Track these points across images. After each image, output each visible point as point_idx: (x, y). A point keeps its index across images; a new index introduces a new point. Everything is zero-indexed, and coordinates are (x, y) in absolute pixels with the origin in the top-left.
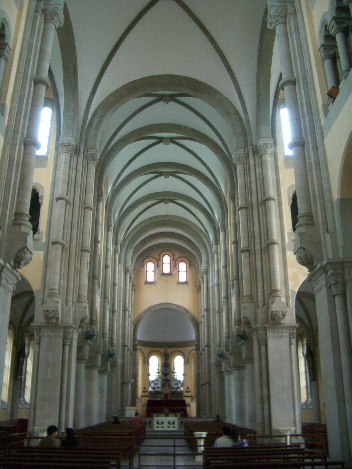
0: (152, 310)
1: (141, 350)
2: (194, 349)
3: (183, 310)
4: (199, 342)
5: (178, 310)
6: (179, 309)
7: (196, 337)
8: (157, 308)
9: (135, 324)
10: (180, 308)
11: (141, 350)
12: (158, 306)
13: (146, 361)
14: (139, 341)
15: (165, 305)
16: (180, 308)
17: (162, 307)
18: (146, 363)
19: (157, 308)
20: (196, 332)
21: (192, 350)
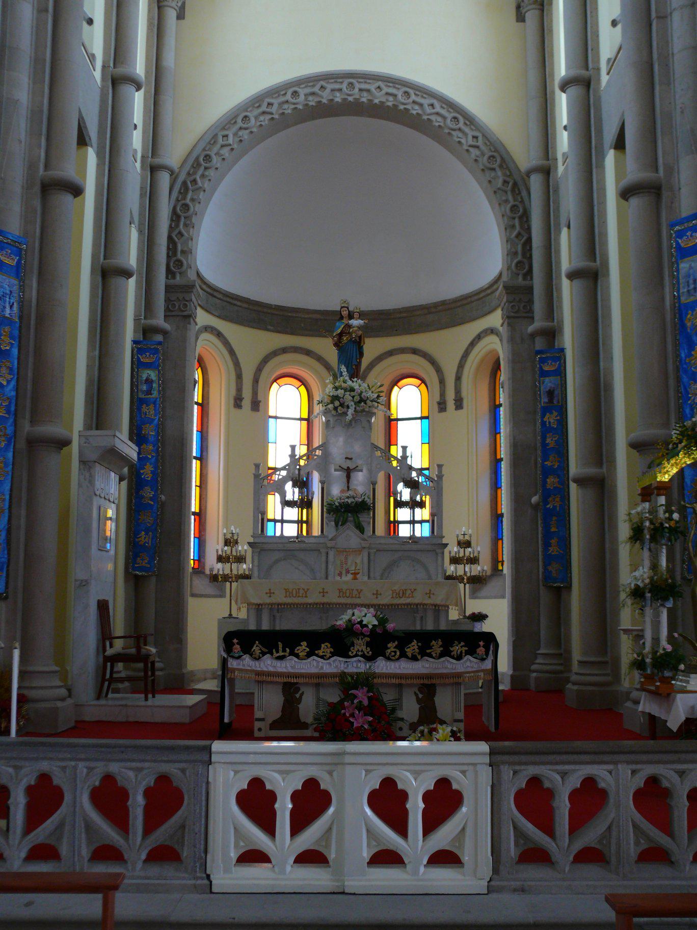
0: (274, 109)
1: (219, 335)
2: (492, 331)
3: (438, 108)
4: (529, 273)
5: (415, 110)
6: (421, 105)
7: (511, 254)
8: (302, 98)
9: (184, 183)
10: (426, 102)
11: (219, 335)
12: (302, 92)
13: (247, 394)
14: (213, 291)
15: (344, 86)
16: (426, 102)
17: (325, 97)
18: (247, 403)
19: (302, 98)
20: (509, 227)
21: (479, 337)
